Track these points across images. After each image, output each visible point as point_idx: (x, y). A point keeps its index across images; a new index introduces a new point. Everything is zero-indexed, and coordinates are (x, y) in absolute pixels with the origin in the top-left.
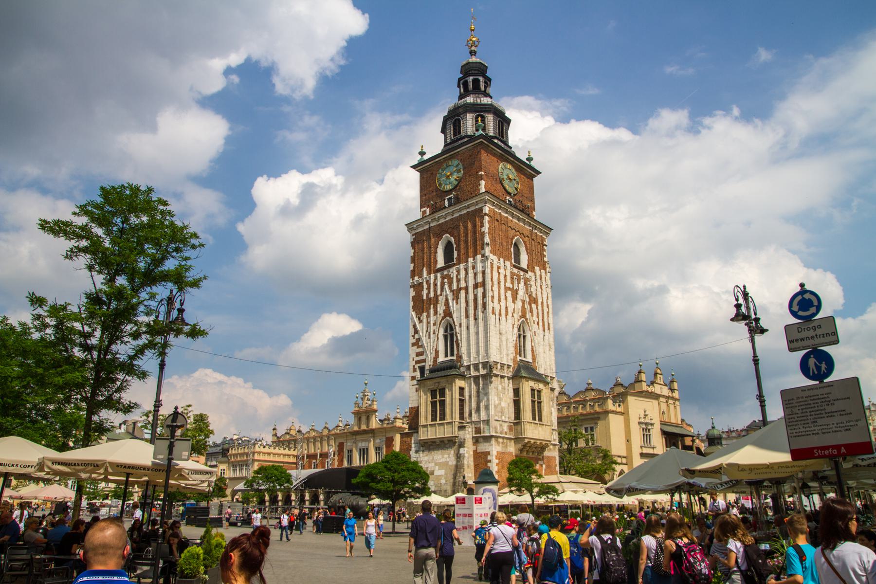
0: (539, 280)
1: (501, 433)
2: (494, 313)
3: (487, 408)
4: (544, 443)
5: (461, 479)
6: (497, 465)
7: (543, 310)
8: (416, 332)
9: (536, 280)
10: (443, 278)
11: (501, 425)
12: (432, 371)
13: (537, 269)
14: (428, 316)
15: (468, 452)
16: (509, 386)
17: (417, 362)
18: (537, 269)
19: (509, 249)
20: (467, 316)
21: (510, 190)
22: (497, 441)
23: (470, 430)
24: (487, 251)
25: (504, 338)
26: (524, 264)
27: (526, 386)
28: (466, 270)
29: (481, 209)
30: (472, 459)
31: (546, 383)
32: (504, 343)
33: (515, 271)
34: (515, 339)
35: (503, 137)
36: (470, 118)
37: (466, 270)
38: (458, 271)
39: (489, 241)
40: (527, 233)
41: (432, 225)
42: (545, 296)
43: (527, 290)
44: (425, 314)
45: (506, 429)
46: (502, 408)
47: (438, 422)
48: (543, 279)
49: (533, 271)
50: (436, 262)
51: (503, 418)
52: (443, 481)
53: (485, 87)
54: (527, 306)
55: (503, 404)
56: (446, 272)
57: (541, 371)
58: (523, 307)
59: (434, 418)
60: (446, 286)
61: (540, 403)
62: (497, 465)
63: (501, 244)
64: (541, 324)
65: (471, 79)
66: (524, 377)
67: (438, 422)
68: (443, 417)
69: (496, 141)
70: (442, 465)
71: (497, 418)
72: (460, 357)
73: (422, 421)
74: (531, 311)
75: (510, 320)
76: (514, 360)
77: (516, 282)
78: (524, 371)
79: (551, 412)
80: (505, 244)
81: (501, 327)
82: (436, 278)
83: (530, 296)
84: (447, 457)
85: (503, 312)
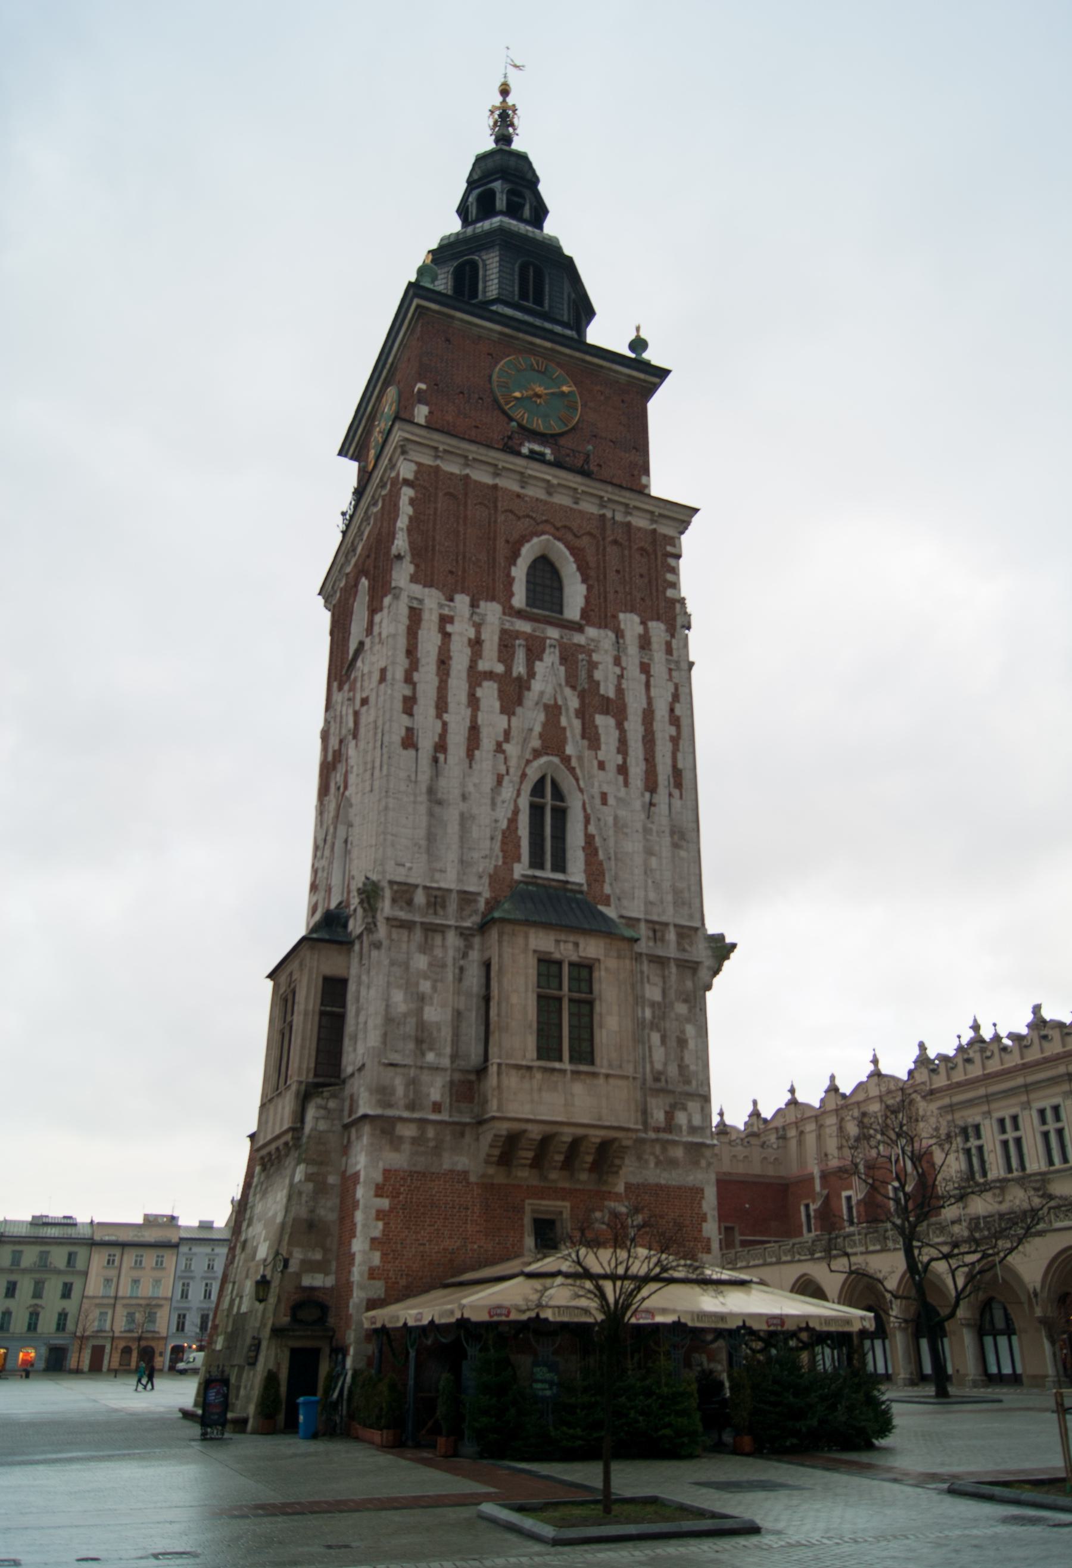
1: (411, 1106)
2: (409, 741)
6: (380, 1215)
11: (413, 1083)
25: (452, 816)
26: (573, 609)
33: (525, 627)
34: (503, 814)
35: (539, 301)
46: (421, 1025)
54: (571, 724)
55: (432, 1014)
62: (380, 1215)
66: (503, 920)
71: (396, 1058)
77: (520, 656)
81: (442, 782)
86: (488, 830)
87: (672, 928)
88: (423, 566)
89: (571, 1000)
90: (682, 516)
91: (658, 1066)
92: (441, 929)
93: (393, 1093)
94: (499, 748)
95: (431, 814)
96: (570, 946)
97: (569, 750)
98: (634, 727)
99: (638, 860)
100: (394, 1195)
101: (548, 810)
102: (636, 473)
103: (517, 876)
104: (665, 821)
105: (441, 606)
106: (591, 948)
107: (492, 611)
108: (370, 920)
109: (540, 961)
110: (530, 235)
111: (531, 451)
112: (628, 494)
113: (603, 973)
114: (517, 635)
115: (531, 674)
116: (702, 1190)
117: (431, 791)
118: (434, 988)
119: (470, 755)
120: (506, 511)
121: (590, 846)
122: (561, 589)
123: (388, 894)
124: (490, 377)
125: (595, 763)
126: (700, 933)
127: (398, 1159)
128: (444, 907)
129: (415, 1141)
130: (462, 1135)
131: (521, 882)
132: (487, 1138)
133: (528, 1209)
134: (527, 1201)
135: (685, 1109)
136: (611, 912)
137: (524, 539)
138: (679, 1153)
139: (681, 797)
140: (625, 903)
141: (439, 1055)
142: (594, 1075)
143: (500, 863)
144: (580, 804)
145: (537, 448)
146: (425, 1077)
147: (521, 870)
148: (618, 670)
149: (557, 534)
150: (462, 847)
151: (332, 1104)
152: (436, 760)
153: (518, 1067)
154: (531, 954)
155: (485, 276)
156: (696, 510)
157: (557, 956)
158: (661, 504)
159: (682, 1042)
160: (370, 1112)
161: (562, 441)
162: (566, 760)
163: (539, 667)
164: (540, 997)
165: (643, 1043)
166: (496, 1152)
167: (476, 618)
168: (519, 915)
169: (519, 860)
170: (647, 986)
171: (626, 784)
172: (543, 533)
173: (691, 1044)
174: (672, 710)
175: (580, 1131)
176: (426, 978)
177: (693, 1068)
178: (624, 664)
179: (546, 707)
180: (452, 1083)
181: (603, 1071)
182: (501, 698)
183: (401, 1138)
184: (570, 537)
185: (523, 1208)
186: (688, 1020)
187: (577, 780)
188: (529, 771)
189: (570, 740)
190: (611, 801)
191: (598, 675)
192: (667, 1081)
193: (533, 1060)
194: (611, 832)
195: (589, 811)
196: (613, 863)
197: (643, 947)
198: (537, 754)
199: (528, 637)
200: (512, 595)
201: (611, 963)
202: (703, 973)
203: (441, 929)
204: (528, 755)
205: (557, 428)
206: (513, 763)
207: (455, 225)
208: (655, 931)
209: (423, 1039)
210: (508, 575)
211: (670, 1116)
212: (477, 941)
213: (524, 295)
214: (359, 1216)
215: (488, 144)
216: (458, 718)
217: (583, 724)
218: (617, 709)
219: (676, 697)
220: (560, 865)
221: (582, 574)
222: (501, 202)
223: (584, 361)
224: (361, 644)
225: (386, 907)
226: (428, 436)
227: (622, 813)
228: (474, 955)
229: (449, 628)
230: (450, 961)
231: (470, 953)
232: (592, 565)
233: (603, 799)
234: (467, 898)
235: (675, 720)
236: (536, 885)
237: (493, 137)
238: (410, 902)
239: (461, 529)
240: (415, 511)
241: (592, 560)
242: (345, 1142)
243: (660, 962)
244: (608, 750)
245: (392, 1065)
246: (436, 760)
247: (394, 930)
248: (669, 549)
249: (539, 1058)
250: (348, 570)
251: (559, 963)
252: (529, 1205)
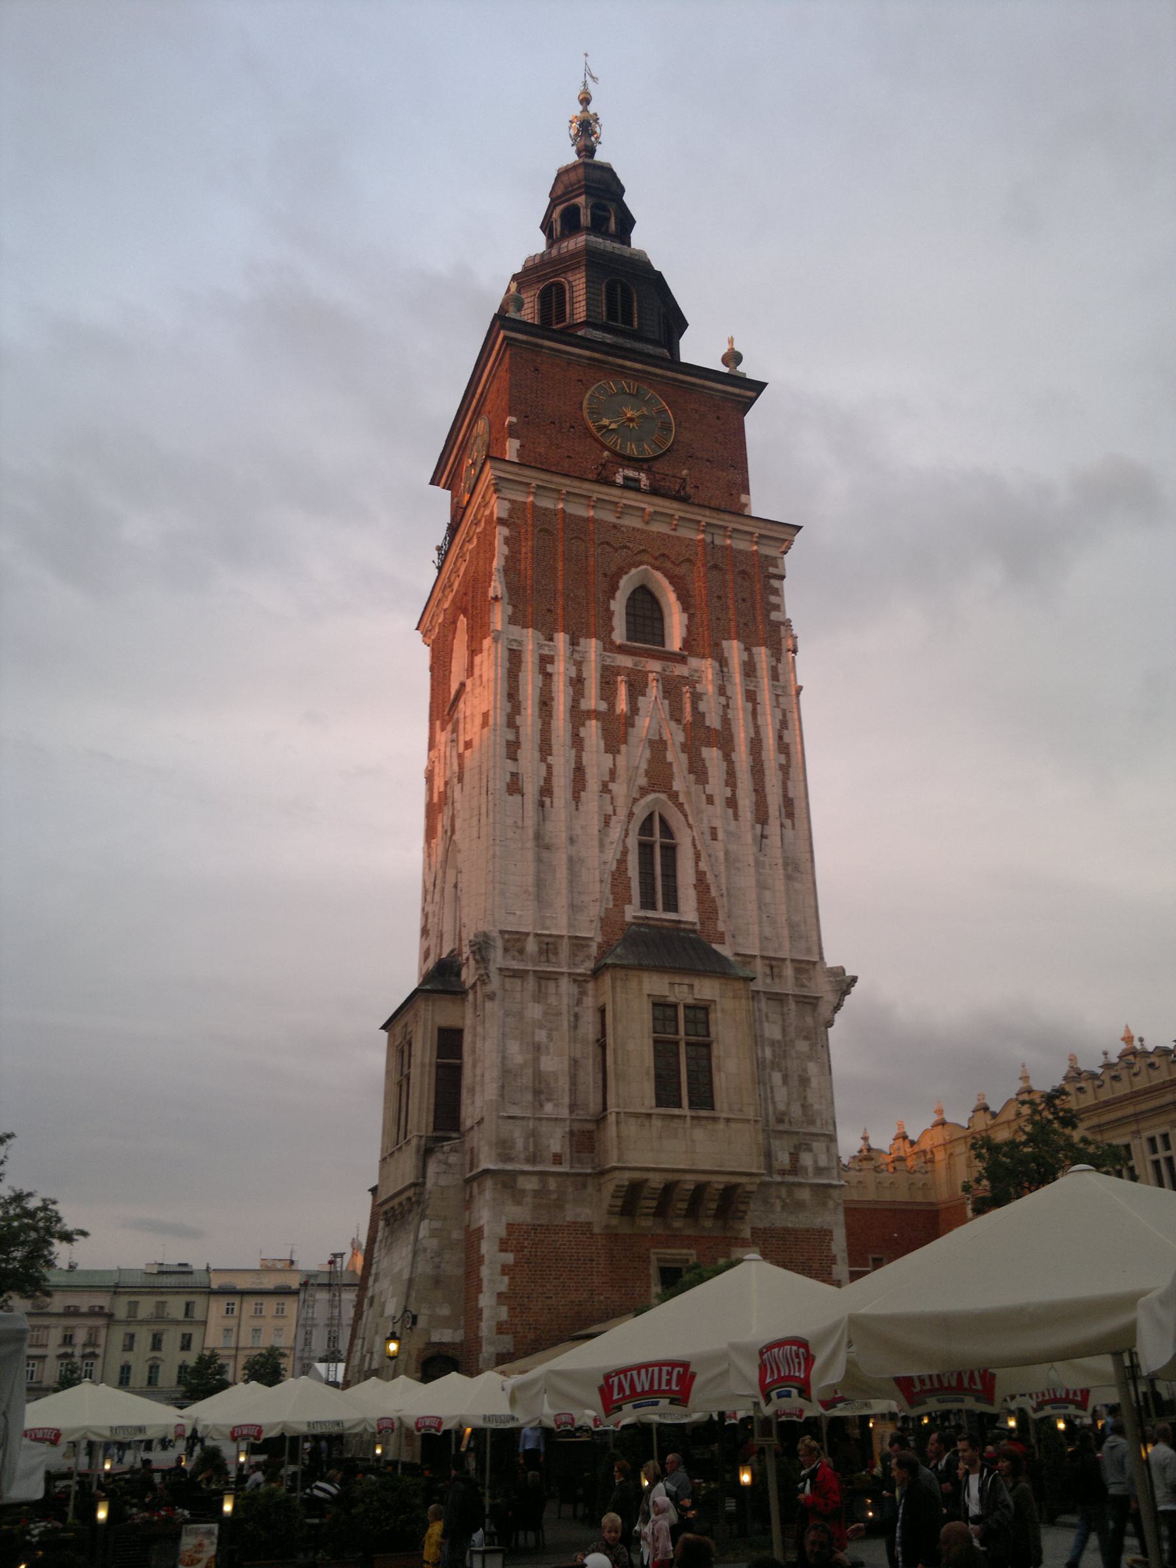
0: (737, 677)
2: (514, 786)
4: (724, 1179)
11: (534, 1134)
25: (560, 859)
26: (675, 642)
33: (626, 661)
34: (611, 855)
35: (628, 320)
45: (556, 1142)
46: (538, 1075)
54: (677, 758)
66: (614, 966)
71: (515, 1111)
74: (698, 771)
76: (605, 922)
77: (623, 690)
81: (549, 826)
86: (597, 873)
87: (788, 963)
88: (521, 607)
89: (688, 1044)
90: (783, 534)
91: (781, 1107)
92: (554, 977)
94: (605, 789)
95: (539, 860)
96: (685, 988)
97: (677, 785)
99: (752, 895)
100: (518, 1250)
101: (656, 848)
102: (734, 492)
104: (777, 853)
105: (540, 646)
106: (707, 989)
107: (592, 647)
108: (482, 972)
109: (654, 1004)
110: (616, 251)
111: (626, 478)
112: (726, 517)
113: (719, 1015)
114: (618, 671)
115: (634, 709)
116: (831, 1232)
117: (538, 836)
118: (550, 1037)
119: (576, 798)
120: (602, 543)
122: (661, 619)
123: (499, 943)
124: (581, 403)
125: (704, 797)
126: (818, 967)
127: (520, 1213)
128: (556, 954)
129: (536, 1193)
130: (584, 1186)
131: (633, 924)
132: (609, 1188)
133: (653, 1258)
134: (653, 1250)
135: (810, 1150)
136: (725, 951)
137: (622, 571)
138: (805, 1195)
139: (793, 828)
140: (740, 940)
141: (556, 1105)
143: (611, 906)
144: (689, 841)
145: (631, 473)
146: (544, 1128)
148: (723, 700)
149: (657, 563)
150: (571, 892)
151: (453, 1159)
152: (542, 804)
153: (636, 1115)
154: (645, 998)
155: (572, 298)
156: (799, 528)
157: (672, 999)
158: (762, 525)
159: (804, 1081)
160: (491, 1167)
161: (657, 466)
162: (674, 796)
163: (642, 702)
164: (656, 1042)
165: (764, 1084)
166: (619, 1202)
167: (577, 656)
168: (631, 960)
169: (630, 902)
170: (766, 1025)
171: (736, 817)
172: (641, 563)
173: (814, 1083)
174: (780, 738)
176: (541, 1027)
177: (816, 1107)
178: (729, 694)
179: (651, 743)
180: (571, 1133)
181: (724, 1115)
183: (523, 1191)
184: (669, 565)
185: (649, 1257)
186: (810, 1058)
187: (686, 816)
188: (636, 810)
189: (676, 775)
191: (702, 707)
192: (790, 1122)
193: (651, 1108)
194: (722, 868)
195: (699, 848)
196: (725, 899)
197: (758, 985)
198: (644, 792)
200: (612, 630)
201: (728, 1004)
202: (824, 1009)
203: (554, 977)
204: (636, 795)
205: (649, 451)
206: (621, 802)
207: (538, 244)
208: (772, 967)
209: (540, 1090)
210: (608, 609)
211: (794, 1157)
213: (612, 315)
214: (485, 1272)
215: (570, 157)
217: (690, 759)
218: (724, 740)
219: (784, 724)
220: (672, 904)
222: (585, 218)
223: (675, 380)
224: (463, 685)
225: (498, 958)
226: (520, 472)
227: (733, 847)
228: (589, 1001)
229: (549, 668)
230: (564, 1009)
231: (585, 999)
233: (710, 837)
234: (579, 943)
235: (783, 748)
236: (648, 926)
237: (575, 148)
238: (521, 951)
240: (511, 551)
242: (468, 1196)
243: (778, 998)
244: (716, 784)
245: (510, 1117)
246: (542, 804)
247: (507, 980)
248: (771, 570)
249: (659, 1104)
250: (446, 606)
251: (675, 1006)
252: (655, 1254)
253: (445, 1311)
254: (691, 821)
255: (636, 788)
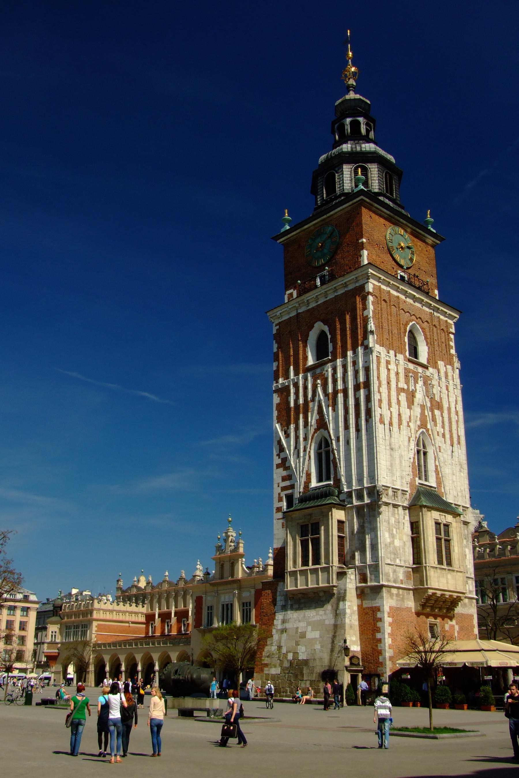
0: (443, 379)
2: (382, 422)
3: (374, 547)
4: (455, 595)
5: (342, 643)
6: (390, 624)
7: (450, 419)
8: (282, 449)
9: (440, 379)
10: (315, 379)
11: (395, 571)
12: (302, 500)
13: (441, 364)
14: (297, 429)
15: (351, 606)
16: (404, 519)
17: (284, 489)
18: (441, 364)
19: (401, 339)
20: (347, 427)
21: (402, 262)
22: (389, 592)
23: (353, 577)
24: (372, 340)
25: (396, 455)
26: (423, 358)
27: (430, 519)
28: (345, 367)
29: (362, 288)
30: (356, 617)
31: (456, 515)
32: (397, 461)
33: (411, 366)
34: (412, 456)
35: (392, 194)
36: (347, 170)
37: (345, 367)
38: (335, 369)
39: (373, 328)
40: (426, 318)
41: (300, 311)
42: (452, 400)
43: (427, 391)
44: (292, 426)
45: (401, 576)
46: (395, 547)
47: (311, 566)
48: (450, 377)
49: (436, 366)
50: (306, 358)
51: (398, 562)
52: (318, 647)
53: (368, 131)
56: (318, 371)
57: (450, 499)
58: (423, 413)
59: (305, 562)
60: (320, 390)
61: (448, 541)
62: (390, 624)
63: (390, 332)
64: (448, 436)
65: (348, 120)
67: (311, 566)
68: (317, 561)
69: (381, 198)
70: (315, 625)
71: (389, 561)
72: (338, 481)
73: (290, 566)
74: (434, 419)
75: (405, 431)
76: (412, 484)
77: (412, 381)
78: (425, 499)
79: (464, 553)
80: (395, 331)
81: (393, 440)
82: (306, 379)
83: (432, 399)
84: (322, 615)
85: (395, 420)
86: (408, 463)
89: (445, 540)
93: (389, 576)
97: (429, 426)
98: (446, 415)
103: (417, 484)
106: (449, 518)
115: (416, 390)
117: (390, 445)
118: (396, 532)
119: (399, 428)
121: (437, 472)
128: (397, 497)
138: (466, 601)
142: (453, 571)
147: (418, 481)
149: (417, 321)
157: (440, 521)
160: (384, 583)
162: (428, 430)
172: (413, 320)
174: (456, 408)
175: (451, 593)
177: (468, 566)
179: (421, 405)
181: (456, 570)
182: (407, 401)
183: (393, 594)
189: (428, 421)
190: (442, 451)
191: (435, 391)
199: (414, 372)
204: (417, 429)
206: (413, 431)
212: (407, 511)
216: (395, 409)
221: (427, 342)
227: (445, 456)
232: (429, 337)
236: (423, 488)
239: (389, 317)
241: (428, 334)
253: (354, 639)
254: (433, 443)
255: (417, 426)
